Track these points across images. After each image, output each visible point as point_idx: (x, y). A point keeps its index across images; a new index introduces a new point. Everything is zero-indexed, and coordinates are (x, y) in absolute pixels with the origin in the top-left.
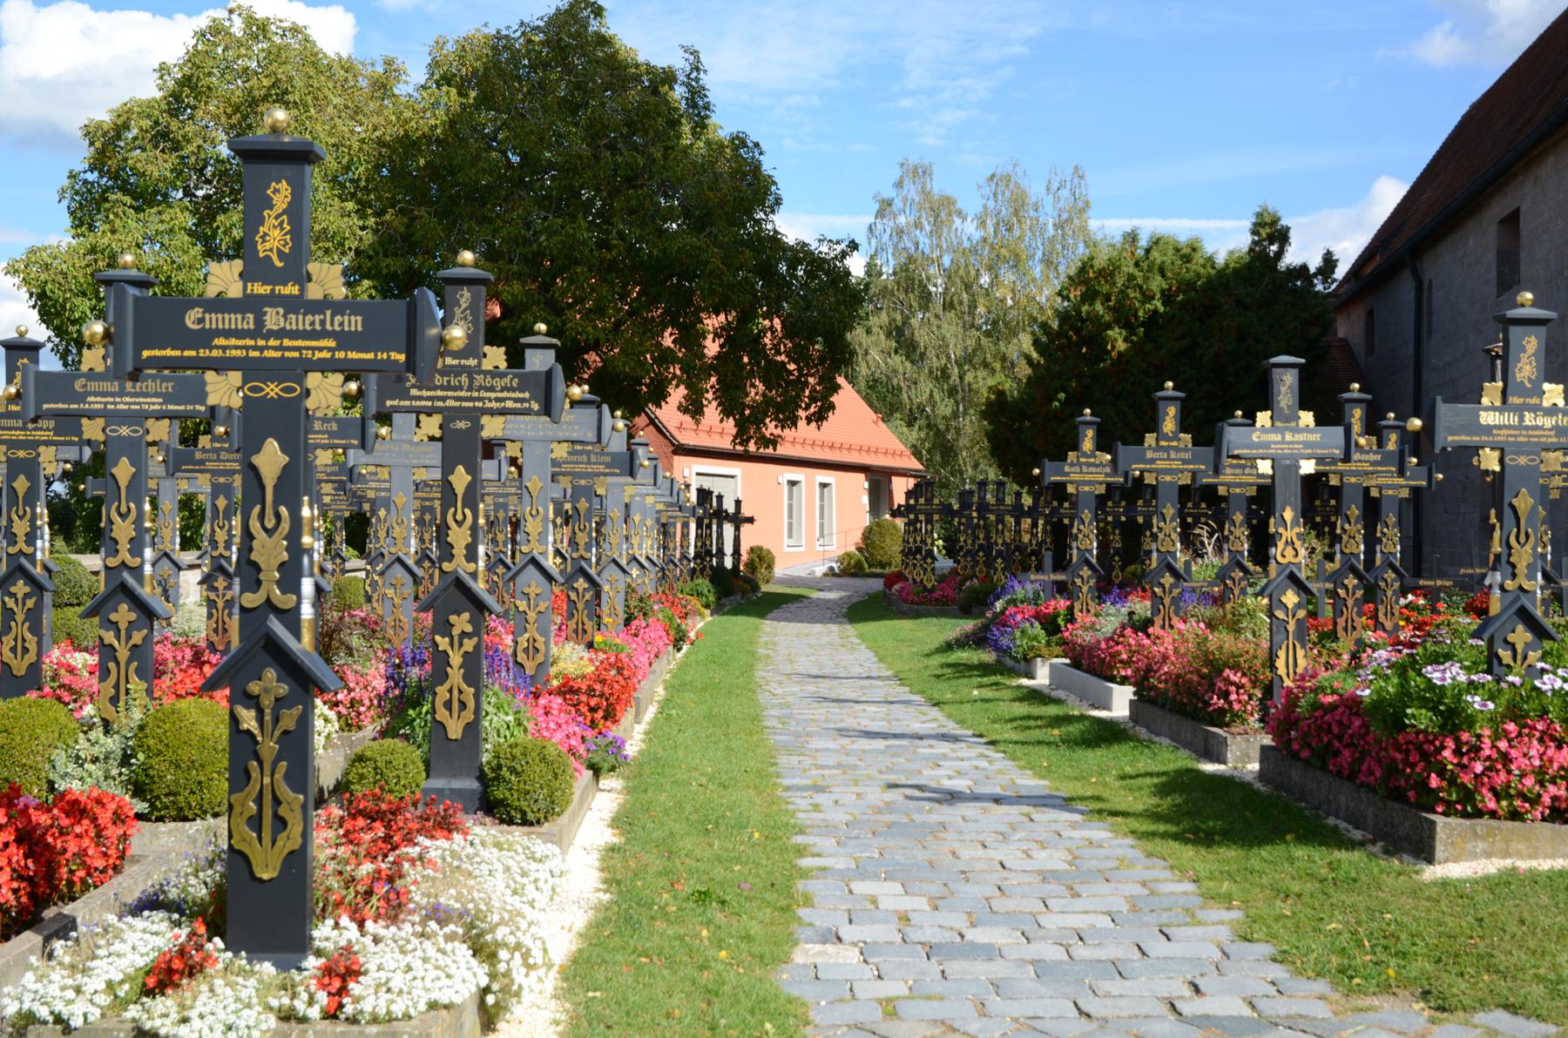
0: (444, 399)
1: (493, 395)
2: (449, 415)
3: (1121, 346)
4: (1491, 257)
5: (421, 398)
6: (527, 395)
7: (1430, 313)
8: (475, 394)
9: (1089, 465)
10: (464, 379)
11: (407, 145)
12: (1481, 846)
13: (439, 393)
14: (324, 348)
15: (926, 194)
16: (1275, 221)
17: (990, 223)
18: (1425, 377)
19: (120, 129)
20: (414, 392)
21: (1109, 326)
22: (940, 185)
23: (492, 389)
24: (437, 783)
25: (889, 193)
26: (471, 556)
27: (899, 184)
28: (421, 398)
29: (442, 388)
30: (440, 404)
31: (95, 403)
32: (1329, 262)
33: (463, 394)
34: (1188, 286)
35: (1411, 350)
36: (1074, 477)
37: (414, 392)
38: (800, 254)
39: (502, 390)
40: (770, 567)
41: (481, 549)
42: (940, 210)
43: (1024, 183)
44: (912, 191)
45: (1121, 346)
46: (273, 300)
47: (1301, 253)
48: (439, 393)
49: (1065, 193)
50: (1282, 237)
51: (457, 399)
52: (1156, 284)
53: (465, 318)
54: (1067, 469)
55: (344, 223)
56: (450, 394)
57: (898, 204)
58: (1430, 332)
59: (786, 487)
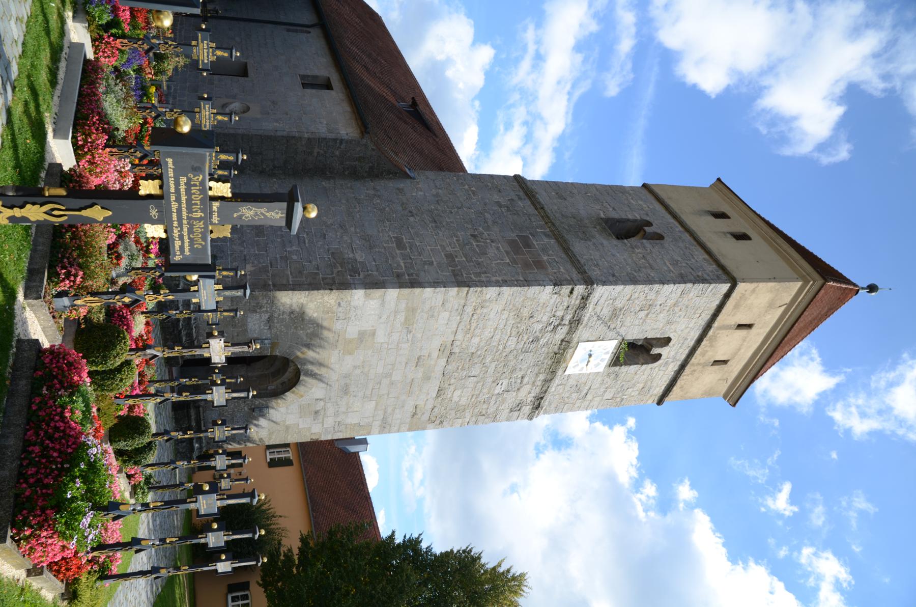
0: (178, 200)
1: (185, 232)
4: (316, 72)
5: (177, 184)
6: (187, 253)
7: (296, 31)
8: (185, 222)
9: (208, 53)
10: (199, 214)
13: (184, 198)
18: (270, 26)
20: (183, 180)
23: (190, 231)
28: (177, 184)
29: (189, 201)
30: (173, 198)
33: (185, 214)
35: (282, 18)
36: (201, 45)
37: (183, 180)
39: (189, 238)
48: (184, 198)
51: (179, 211)
53: (256, 214)
54: (205, 42)
56: (184, 205)
58: (288, 30)
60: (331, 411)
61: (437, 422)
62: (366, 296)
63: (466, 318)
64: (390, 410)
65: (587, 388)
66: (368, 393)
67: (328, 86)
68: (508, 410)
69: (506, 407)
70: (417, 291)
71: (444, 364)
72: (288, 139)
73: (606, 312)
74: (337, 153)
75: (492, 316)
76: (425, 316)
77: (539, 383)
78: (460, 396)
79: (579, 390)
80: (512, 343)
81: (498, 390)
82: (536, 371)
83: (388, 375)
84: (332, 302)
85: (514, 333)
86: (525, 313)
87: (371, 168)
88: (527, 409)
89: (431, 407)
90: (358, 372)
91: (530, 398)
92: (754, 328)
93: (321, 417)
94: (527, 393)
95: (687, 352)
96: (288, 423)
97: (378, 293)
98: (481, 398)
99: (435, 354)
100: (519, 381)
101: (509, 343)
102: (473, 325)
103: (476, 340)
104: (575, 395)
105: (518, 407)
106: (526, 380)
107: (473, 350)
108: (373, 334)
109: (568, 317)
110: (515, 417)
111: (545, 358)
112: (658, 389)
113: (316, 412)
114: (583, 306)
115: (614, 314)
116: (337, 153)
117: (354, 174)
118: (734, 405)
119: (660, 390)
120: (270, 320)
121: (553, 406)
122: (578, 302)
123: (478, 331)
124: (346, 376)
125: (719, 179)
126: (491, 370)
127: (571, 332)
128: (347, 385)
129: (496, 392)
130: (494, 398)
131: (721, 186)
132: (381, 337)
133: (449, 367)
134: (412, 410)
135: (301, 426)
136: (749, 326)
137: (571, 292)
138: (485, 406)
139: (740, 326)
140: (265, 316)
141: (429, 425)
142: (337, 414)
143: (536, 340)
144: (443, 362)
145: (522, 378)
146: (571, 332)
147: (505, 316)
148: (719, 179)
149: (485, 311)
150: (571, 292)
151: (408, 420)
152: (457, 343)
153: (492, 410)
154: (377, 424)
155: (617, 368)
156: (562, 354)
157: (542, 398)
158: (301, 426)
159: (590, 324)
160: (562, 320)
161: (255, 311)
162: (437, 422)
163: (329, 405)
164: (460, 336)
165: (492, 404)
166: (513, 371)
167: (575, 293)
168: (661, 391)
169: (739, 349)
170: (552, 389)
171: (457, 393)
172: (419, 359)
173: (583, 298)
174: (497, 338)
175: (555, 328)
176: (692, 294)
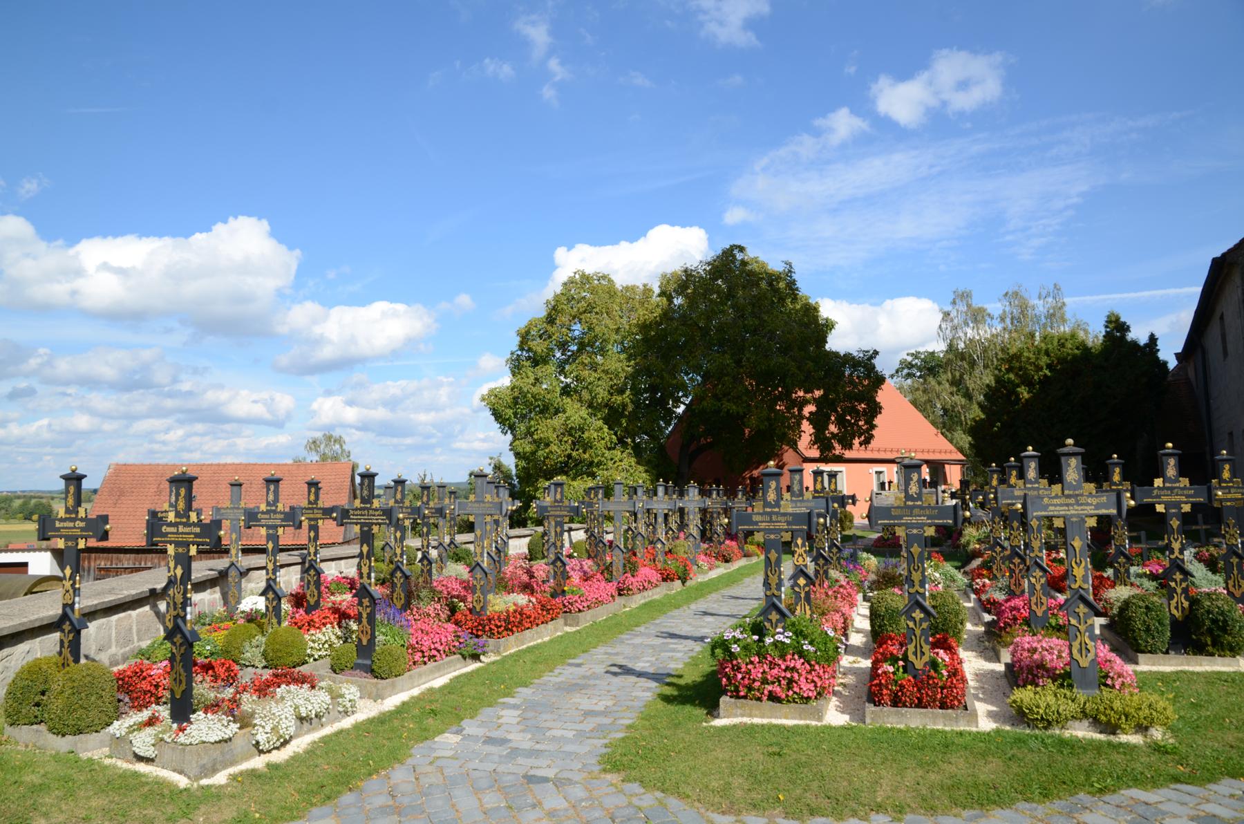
2: (363, 525)
3: (1026, 395)
11: (644, 327)
12: (739, 711)
14: (191, 538)
15: (969, 306)
16: (1118, 319)
17: (1008, 321)
19: (528, 333)
21: (1018, 386)
22: (976, 303)
24: (360, 661)
25: (948, 308)
26: (369, 577)
27: (954, 303)
31: (263, 522)
34: (1062, 360)
38: (848, 359)
40: (851, 521)
41: (373, 575)
42: (977, 316)
43: (1026, 295)
45: (1026, 395)
46: (181, 523)
52: (1044, 360)
55: (619, 365)
57: (953, 314)
59: (875, 476)
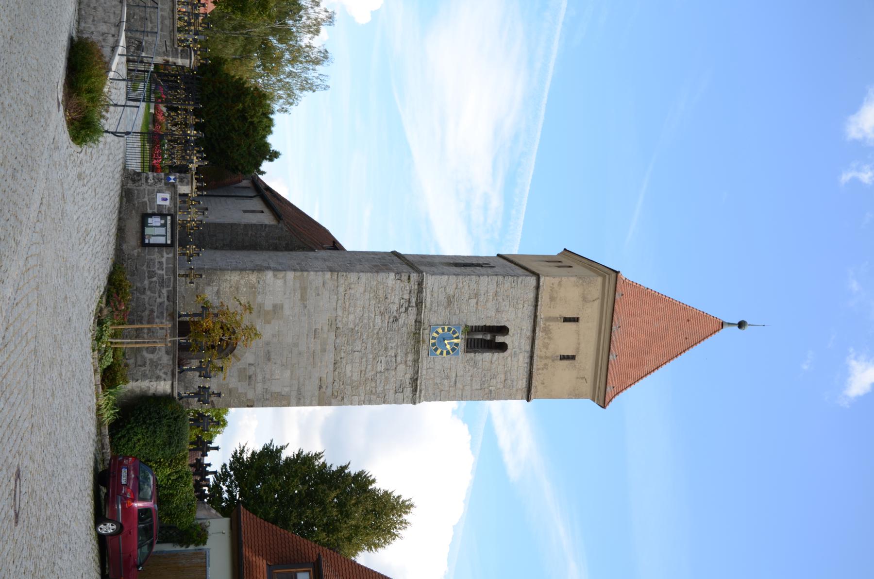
22: (324, 29)
32: (263, 173)
44: (323, 15)
47: (265, 166)
49: (319, 82)
50: (271, 160)
60: (260, 377)
61: (339, 398)
62: (275, 276)
63: (341, 297)
64: (301, 380)
65: (454, 375)
66: (284, 361)
67: (262, 212)
68: (392, 392)
69: (391, 387)
70: (305, 274)
71: (334, 337)
72: (232, 225)
73: (442, 298)
74: (264, 234)
75: (358, 295)
76: (314, 294)
77: (410, 363)
78: (351, 371)
79: (448, 377)
80: (378, 320)
81: (381, 367)
82: (404, 350)
83: (296, 345)
84: (254, 280)
85: (378, 312)
86: (381, 294)
87: (287, 244)
88: (408, 391)
89: (331, 380)
90: (275, 340)
91: (407, 379)
92: (580, 321)
93: (253, 382)
94: (404, 373)
95: (529, 342)
96: (230, 386)
97: (281, 275)
98: (370, 375)
99: (326, 328)
100: (394, 359)
101: (376, 321)
102: (347, 304)
103: (351, 317)
104: (445, 382)
105: (400, 389)
106: (399, 359)
107: (351, 326)
108: (282, 307)
109: (414, 300)
110: (401, 400)
111: (408, 339)
112: (520, 382)
113: (250, 377)
114: (420, 290)
115: (450, 301)
116: (264, 234)
117: (276, 248)
118: (604, 407)
119: (523, 384)
120: (218, 292)
121: (431, 392)
122: (416, 287)
123: (352, 309)
124: (268, 344)
125: (565, 249)
126: (369, 345)
127: (419, 313)
128: (269, 352)
129: (379, 370)
130: (378, 375)
131: (566, 253)
132: (287, 311)
133: (338, 341)
134: (317, 382)
135: (240, 391)
136: (576, 320)
137: (409, 279)
138: (373, 384)
139: (566, 320)
140: (216, 289)
141: (333, 401)
142: (264, 380)
143: (396, 320)
144: (332, 336)
145: (396, 356)
146: (419, 313)
147: (367, 296)
148: (565, 249)
149: (352, 292)
150: (409, 279)
151: (317, 393)
152: (339, 319)
153: (380, 389)
154: (294, 394)
155: (472, 355)
156: (419, 334)
157: (417, 379)
158: (240, 391)
159: (433, 309)
160: (409, 302)
161: (209, 285)
162: (339, 398)
163: (258, 370)
164: (340, 313)
165: (378, 381)
166: (386, 349)
167: (412, 279)
168: (524, 385)
169: (579, 344)
170: (423, 372)
171: (349, 368)
172: (315, 331)
173: (419, 284)
174: (366, 315)
175: (407, 309)
176: (506, 286)
